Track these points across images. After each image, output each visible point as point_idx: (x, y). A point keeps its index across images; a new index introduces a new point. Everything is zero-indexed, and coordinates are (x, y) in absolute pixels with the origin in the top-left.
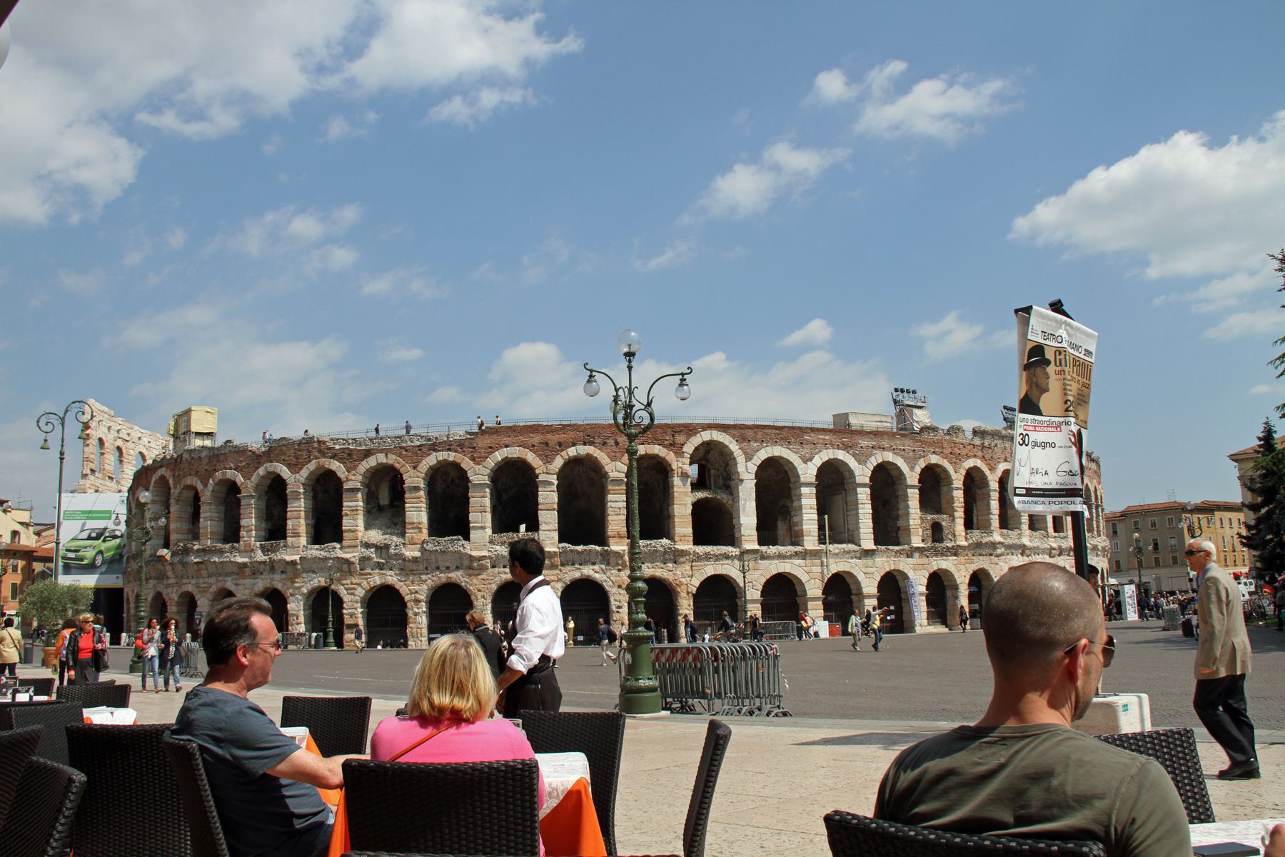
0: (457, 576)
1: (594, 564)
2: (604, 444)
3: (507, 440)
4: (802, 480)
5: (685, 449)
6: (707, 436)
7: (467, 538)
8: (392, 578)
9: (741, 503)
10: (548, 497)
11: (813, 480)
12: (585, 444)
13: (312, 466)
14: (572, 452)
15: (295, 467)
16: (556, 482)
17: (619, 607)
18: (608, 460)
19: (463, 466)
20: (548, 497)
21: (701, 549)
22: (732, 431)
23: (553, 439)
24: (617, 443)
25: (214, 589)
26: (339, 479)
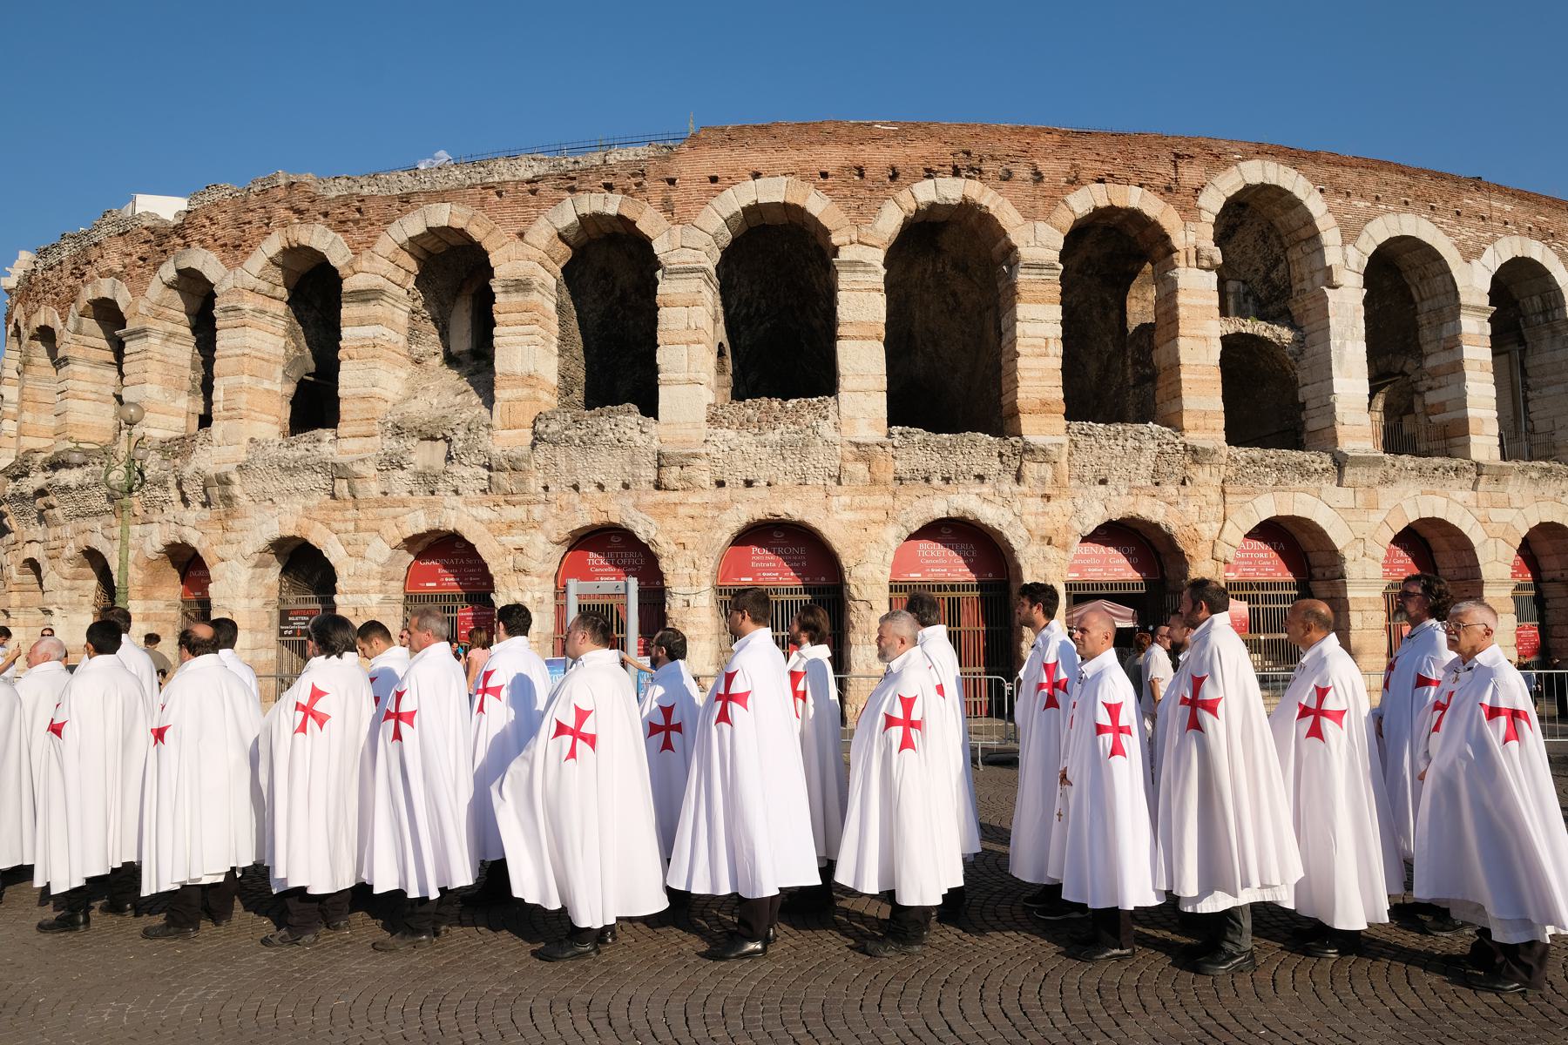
0: (620, 510)
1: (981, 478)
2: (1008, 176)
3: (756, 160)
4: (1463, 299)
5: (1203, 200)
6: (1257, 172)
7: (649, 408)
8: (464, 515)
9: (1335, 342)
10: (861, 305)
11: (1485, 301)
12: (956, 173)
13: (274, 245)
14: (926, 192)
15: (235, 250)
16: (884, 272)
18: (1020, 220)
19: (643, 226)
20: (861, 305)
21: (1241, 453)
22: (1310, 167)
23: (878, 157)
24: (1038, 177)
25: (71, 550)
26: (335, 271)
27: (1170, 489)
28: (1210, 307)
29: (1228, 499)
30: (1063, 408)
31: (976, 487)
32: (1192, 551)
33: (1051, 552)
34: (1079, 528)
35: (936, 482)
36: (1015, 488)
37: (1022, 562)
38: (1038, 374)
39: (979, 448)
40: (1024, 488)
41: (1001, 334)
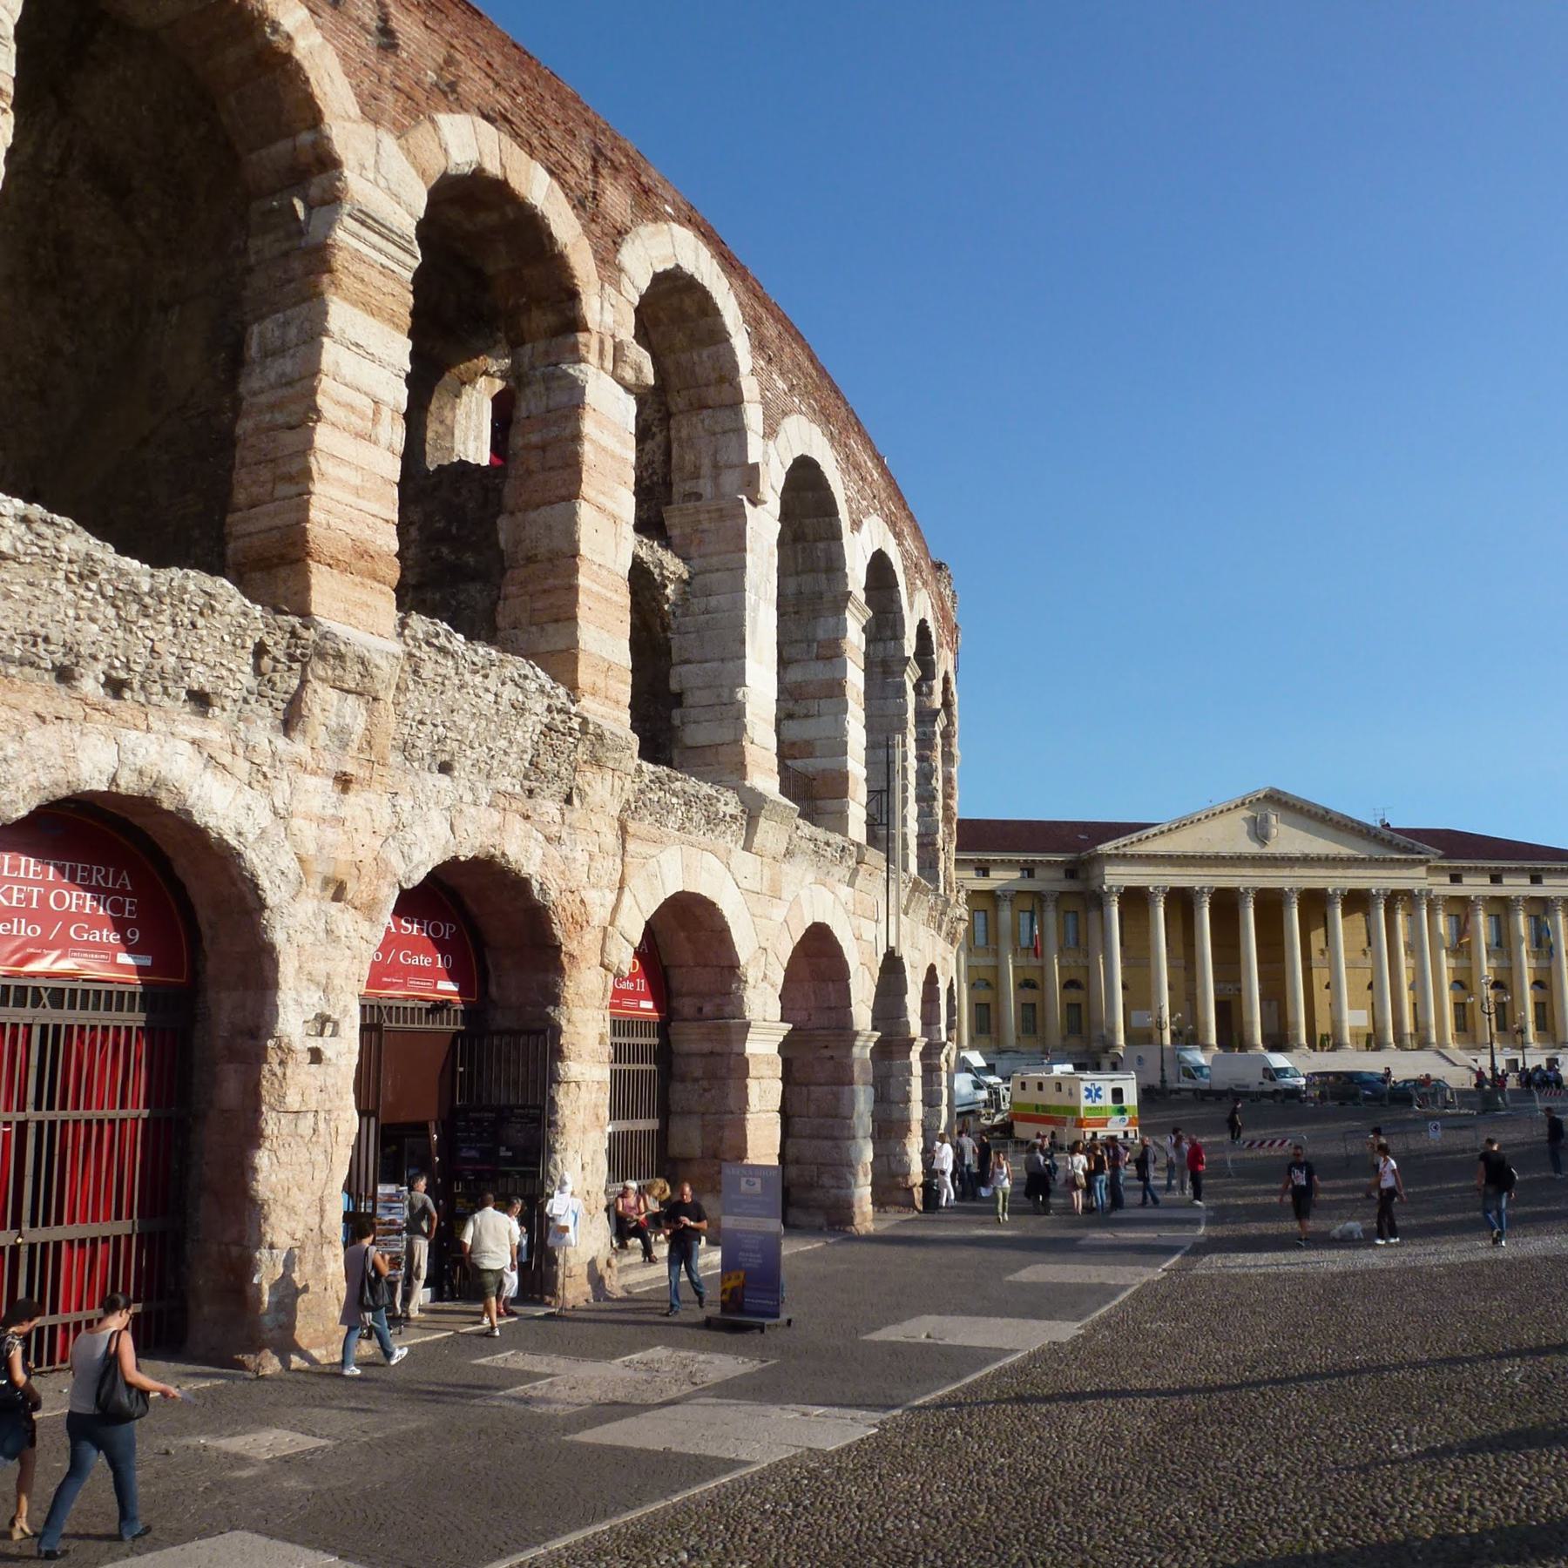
1: (201, 700)
17: (323, 1020)
18: (355, 111)
27: (550, 807)
28: (624, 460)
29: (631, 846)
30: (394, 574)
31: (190, 726)
32: (570, 946)
33: (345, 920)
34: (401, 869)
35: (90, 685)
36: (281, 742)
37: (278, 937)
38: (355, 479)
39: (213, 616)
40: (299, 748)
41: (236, 362)
